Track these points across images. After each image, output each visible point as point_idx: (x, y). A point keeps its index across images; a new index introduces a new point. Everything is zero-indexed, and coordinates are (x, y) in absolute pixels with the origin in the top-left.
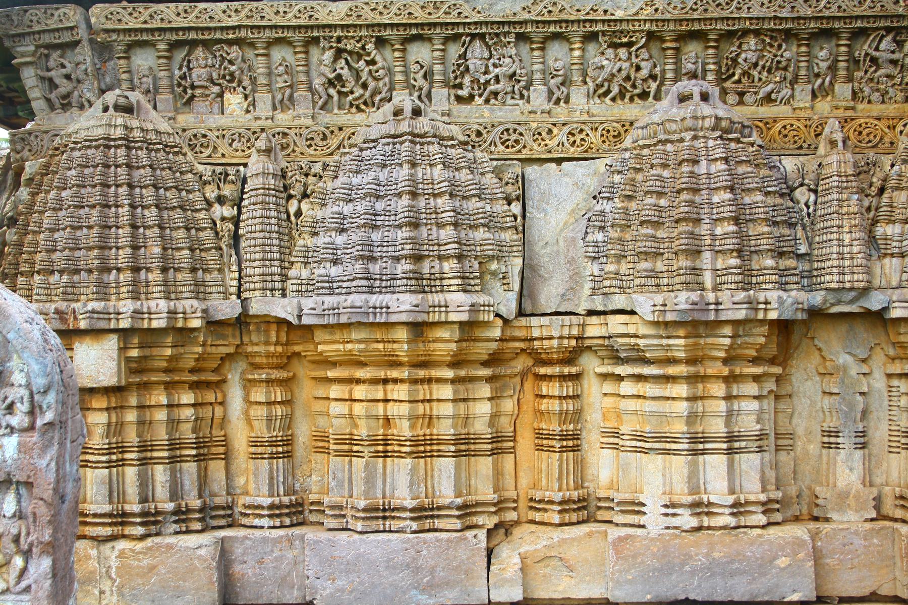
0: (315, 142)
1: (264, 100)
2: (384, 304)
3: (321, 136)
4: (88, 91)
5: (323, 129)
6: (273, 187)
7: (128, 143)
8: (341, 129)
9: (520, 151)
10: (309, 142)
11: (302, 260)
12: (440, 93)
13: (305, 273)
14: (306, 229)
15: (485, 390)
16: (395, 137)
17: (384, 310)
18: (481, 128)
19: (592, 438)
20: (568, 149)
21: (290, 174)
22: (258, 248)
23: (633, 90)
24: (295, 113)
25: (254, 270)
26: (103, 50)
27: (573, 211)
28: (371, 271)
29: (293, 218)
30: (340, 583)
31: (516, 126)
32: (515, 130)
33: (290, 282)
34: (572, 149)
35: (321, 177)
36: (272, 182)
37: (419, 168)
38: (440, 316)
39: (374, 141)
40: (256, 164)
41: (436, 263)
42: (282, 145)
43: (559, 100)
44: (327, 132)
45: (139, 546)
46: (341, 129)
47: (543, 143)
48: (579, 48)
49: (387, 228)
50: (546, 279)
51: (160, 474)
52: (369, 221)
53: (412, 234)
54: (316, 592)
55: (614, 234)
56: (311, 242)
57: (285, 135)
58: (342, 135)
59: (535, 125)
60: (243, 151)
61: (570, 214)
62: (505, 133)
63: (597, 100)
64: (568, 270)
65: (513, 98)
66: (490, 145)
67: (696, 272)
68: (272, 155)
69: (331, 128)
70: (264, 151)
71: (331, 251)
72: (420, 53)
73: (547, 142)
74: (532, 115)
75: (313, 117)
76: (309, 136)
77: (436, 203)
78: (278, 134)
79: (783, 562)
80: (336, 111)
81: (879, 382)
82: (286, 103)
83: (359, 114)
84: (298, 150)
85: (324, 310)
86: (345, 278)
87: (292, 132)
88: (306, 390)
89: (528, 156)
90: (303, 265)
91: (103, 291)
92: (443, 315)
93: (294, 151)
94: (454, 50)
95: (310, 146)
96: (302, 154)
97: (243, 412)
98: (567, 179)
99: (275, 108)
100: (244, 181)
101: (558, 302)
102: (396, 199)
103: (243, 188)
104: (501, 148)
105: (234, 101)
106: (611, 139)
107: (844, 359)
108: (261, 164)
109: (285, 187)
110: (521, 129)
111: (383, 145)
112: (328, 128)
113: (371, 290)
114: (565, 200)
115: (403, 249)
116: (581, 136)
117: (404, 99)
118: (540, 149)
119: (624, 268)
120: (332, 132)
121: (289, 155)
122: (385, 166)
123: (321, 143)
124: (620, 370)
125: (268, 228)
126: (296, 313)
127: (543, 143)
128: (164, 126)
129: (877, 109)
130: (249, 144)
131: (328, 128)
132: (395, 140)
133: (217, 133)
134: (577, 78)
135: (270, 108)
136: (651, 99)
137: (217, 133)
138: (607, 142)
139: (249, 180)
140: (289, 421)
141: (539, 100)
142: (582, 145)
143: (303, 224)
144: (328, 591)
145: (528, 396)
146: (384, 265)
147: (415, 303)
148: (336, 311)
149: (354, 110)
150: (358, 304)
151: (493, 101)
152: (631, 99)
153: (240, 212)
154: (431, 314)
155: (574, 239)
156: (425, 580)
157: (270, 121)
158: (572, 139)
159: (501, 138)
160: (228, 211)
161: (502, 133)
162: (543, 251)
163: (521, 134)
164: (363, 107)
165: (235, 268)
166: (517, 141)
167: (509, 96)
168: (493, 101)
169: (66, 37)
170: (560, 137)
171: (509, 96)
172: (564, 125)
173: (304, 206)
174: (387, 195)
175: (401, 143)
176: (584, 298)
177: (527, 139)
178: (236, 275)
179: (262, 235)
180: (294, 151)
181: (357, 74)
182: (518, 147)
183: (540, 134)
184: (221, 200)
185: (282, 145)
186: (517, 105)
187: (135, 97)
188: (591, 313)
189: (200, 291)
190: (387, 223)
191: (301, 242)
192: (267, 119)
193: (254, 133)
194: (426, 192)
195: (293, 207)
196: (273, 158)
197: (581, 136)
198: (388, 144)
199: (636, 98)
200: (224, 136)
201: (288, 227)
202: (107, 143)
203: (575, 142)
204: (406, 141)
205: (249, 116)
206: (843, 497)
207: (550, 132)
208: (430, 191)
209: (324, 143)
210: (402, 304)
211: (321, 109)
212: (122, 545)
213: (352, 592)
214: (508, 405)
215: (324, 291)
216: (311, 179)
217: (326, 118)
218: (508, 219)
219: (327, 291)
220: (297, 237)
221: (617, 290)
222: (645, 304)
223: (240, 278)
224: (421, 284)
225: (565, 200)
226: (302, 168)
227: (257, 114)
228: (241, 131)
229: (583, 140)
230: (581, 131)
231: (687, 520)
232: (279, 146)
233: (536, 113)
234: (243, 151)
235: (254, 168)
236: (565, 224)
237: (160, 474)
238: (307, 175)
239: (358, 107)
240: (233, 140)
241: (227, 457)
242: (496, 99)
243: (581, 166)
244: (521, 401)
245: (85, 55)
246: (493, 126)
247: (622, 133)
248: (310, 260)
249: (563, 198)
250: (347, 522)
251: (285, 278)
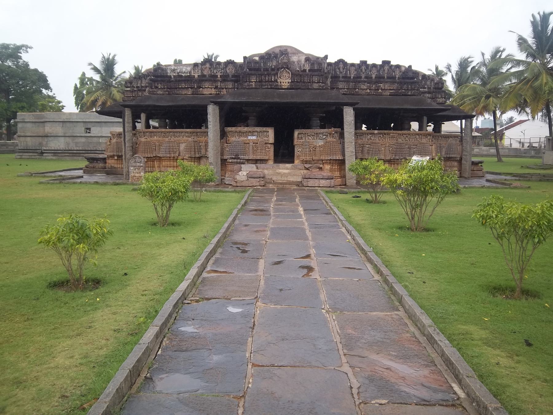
26: (144, 133)
72: (171, 134)
117: (169, 138)
201: (160, 149)
210: (168, 155)
224: (170, 154)
249: (182, 147)
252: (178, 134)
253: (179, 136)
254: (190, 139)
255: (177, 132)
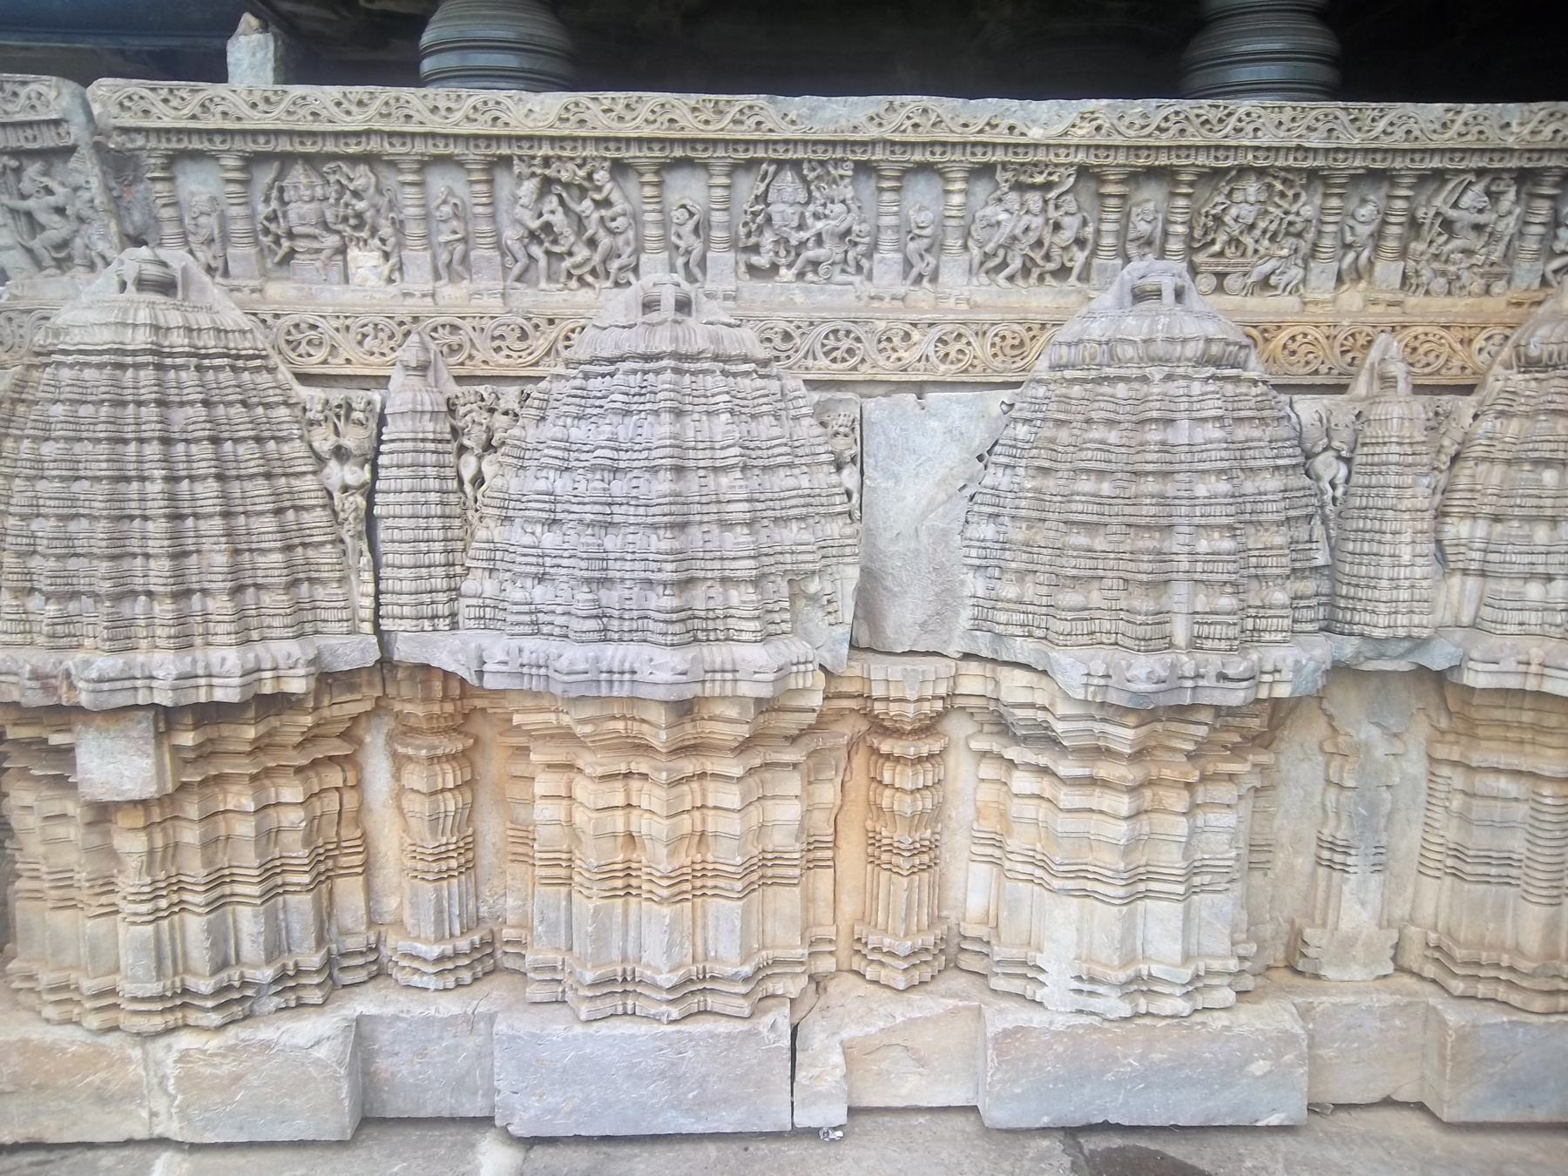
0: (508, 343)
1: (418, 260)
2: (627, 667)
3: (518, 333)
4: (101, 236)
5: (521, 321)
6: (431, 436)
7: (160, 357)
8: (551, 322)
9: (855, 368)
10: (497, 343)
11: (485, 564)
12: (722, 260)
13: (490, 587)
14: (490, 511)
15: (792, 784)
16: (647, 358)
17: (627, 677)
18: (790, 328)
19: (958, 847)
20: (936, 368)
21: (462, 410)
22: (405, 547)
23: (1044, 264)
24: (473, 287)
25: (399, 581)
26: (120, 167)
27: (944, 480)
28: (604, 602)
29: (468, 488)
30: (550, 1100)
31: (851, 326)
32: (848, 332)
33: (464, 602)
34: (942, 368)
35: (516, 415)
36: (430, 426)
37: (687, 420)
38: (722, 688)
39: (612, 361)
40: (402, 394)
41: (717, 590)
42: (450, 346)
43: (921, 276)
44: (528, 327)
45: (214, 1043)
46: (551, 322)
47: (895, 356)
48: (961, 191)
49: (632, 529)
50: (895, 595)
51: (248, 923)
52: (600, 518)
53: (676, 545)
54: (512, 1115)
55: (1018, 534)
56: (499, 533)
57: (455, 328)
58: (554, 332)
59: (882, 325)
60: (383, 354)
61: (938, 485)
62: (831, 337)
63: (984, 279)
64: (933, 583)
65: (843, 271)
66: (805, 357)
67: (1161, 617)
68: (430, 373)
69: (535, 321)
70: (415, 369)
71: (534, 560)
72: (688, 190)
73: (901, 354)
74: (876, 304)
75: (503, 295)
76: (497, 333)
77: (718, 484)
78: (443, 326)
79: (1259, 1067)
80: (543, 284)
81: (1415, 766)
82: (456, 267)
83: (583, 291)
84: (479, 357)
85: (522, 665)
86: (566, 554)
87: (466, 325)
88: (494, 765)
89: (869, 378)
90: (487, 574)
91: (121, 637)
92: (729, 685)
93: (471, 357)
94: (748, 187)
95: (498, 350)
96: (485, 362)
97: (395, 796)
98: (933, 424)
99: (437, 277)
100: (382, 421)
101: (914, 636)
102: (647, 475)
103: (380, 433)
104: (824, 362)
105: (365, 261)
106: (1008, 351)
107: (1369, 732)
108: (409, 396)
109: (455, 431)
110: (858, 331)
111: (626, 373)
112: (529, 319)
113: (604, 637)
114: (930, 459)
115: (660, 570)
116: (958, 346)
117: (657, 276)
118: (889, 365)
119: (1031, 592)
120: (537, 326)
121: (462, 364)
122: (628, 413)
123: (518, 345)
124: (1012, 753)
125: (424, 511)
126: (474, 668)
127: (895, 356)
128: (232, 317)
129: (1439, 303)
130: (392, 343)
131: (529, 319)
132: (647, 366)
133: (336, 323)
134: (954, 242)
135: (429, 276)
136: (1073, 279)
137: (336, 323)
138: (1001, 357)
139: (389, 419)
140: (468, 815)
141: (888, 278)
142: (960, 361)
143: (487, 501)
144: (532, 1112)
145: (859, 779)
146: (627, 593)
147: (680, 668)
148: (543, 671)
149: (574, 284)
150: (582, 667)
151: (810, 276)
152: (1041, 278)
153: (375, 476)
154: (708, 685)
155: (945, 533)
156: (690, 1096)
157: (429, 300)
158: (942, 350)
159: (823, 345)
160: (355, 474)
161: (826, 337)
162: (893, 549)
163: (858, 339)
164: (590, 279)
165: (368, 576)
166: (850, 351)
167: (838, 269)
168: (810, 276)
169: (48, 140)
170: (923, 346)
171: (838, 269)
172: (930, 325)
173: (488, 469)
174: (632, 469)
175: (657, 372)
176: (957, 633)
177: (868, 347)
178: (370, 588)
179: (412, 523)
180: (471, 357)
181: (580, 223)
182: (852, 362)
183: (889, 340)
184: (340, 453)
185: (450, 346)
186: (851, 284)
187: (177, 258)
188: (967, 656)
189: (303, 623)
190: (632, 520)
191: (482, 534)
192: (424, 296)
193: (401, 323)
194: (702, 463)
195: (468, 467)
196: (431, 379)
197: (958, 346)
198: (635, 372)
199: (1048, 277)
200: (348, 328)
201: (459, 502)
202: (119, 360)
203: (947, 355)
204: (665, 369)
205: (392, 289)
206: (1347, 944)
207: (907, 336)
208: (708, 463)
209: (523, 345)
210: (662, 667)
211: (519, 279)
212: (185, 1040)
213: (570, 1113)
214: (827, 793)
215: (521, 629)
216: (500, 420)
217: (525, 297)
218: (838, 499)
219: (528, 629)
220: (475, 521)
221: (1019, 631)
222: (1075, 668)
223: (378, 593)
224: (692, 629)
225: (930, 459)
226: (483, 400)
227: (408, 286)
228: (377, 320)
229: (961, 351)
230: (960, 335)
231: (1113, 1004)
232: (445, 349)
233: (882, 299)
234: (383, 354)
235: (398, 402)
236: (929, 503)
237: (248, 923)
238: (492, 411)
239: (580, 279)
240: (365, 336)
241: (367, 868)
242: (816, 272)
243: (958, 401)
244: (847, 785)
245: (87, 173)
246: (811, 324)
247: (1027, 341)
248: (499, 565)
249: (926, 458)
250: (564, 992)
251: (455, 593)
252: (844, 204)
253: (856, 251)
254: (1097, 313)
255: (808, 162)
